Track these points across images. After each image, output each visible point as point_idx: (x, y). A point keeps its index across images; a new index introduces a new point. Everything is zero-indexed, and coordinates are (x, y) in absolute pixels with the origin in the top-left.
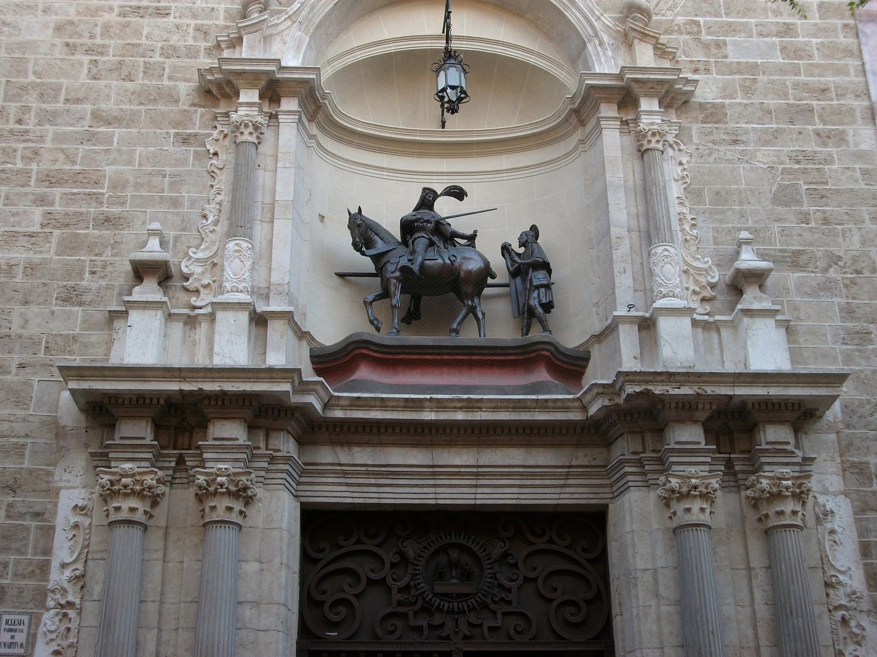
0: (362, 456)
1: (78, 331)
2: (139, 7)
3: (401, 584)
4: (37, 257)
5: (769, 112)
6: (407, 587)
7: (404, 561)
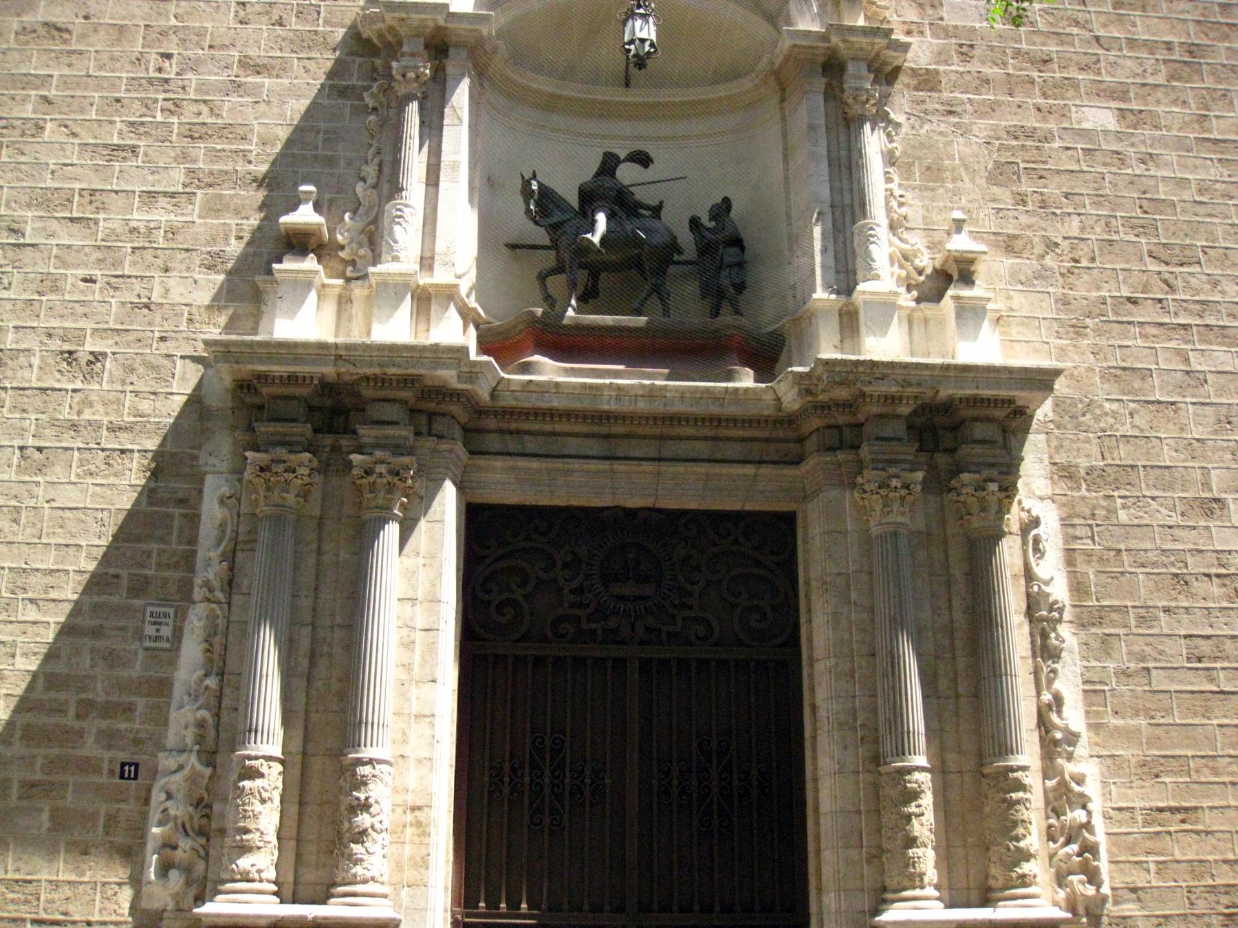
3: (574, 585)
5: (987, 81)
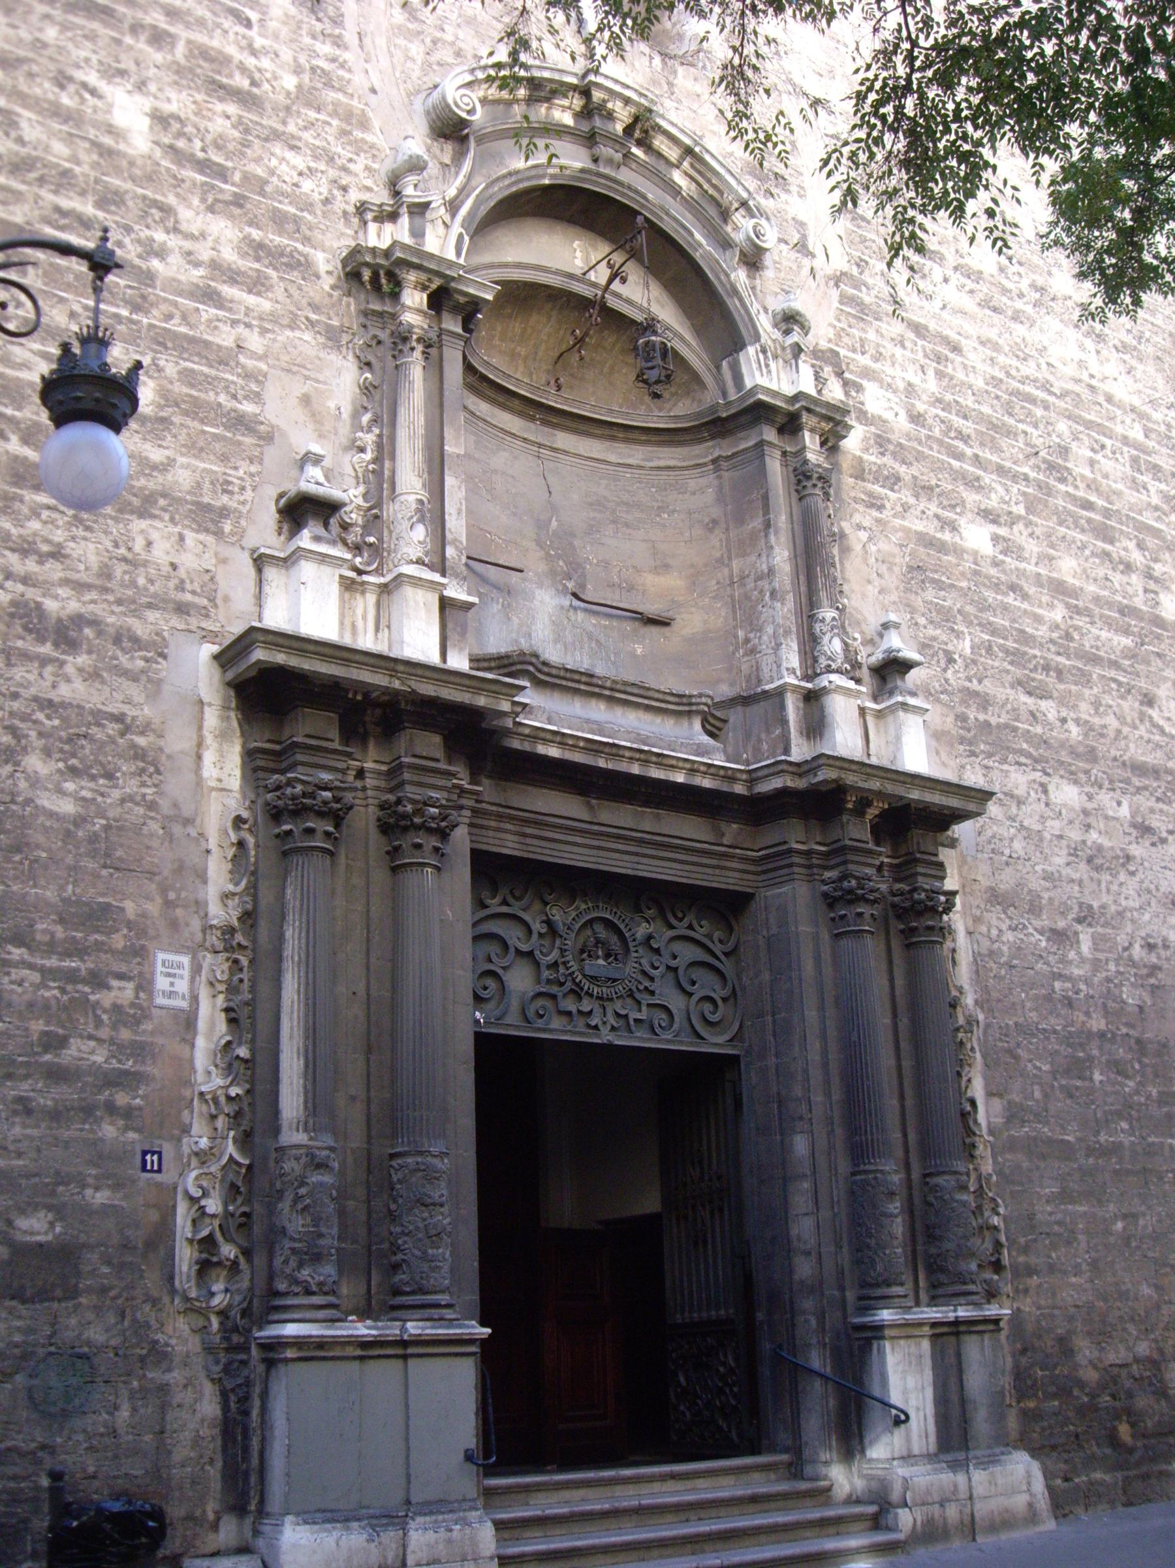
3: (550, 958)
7: (552, 930)
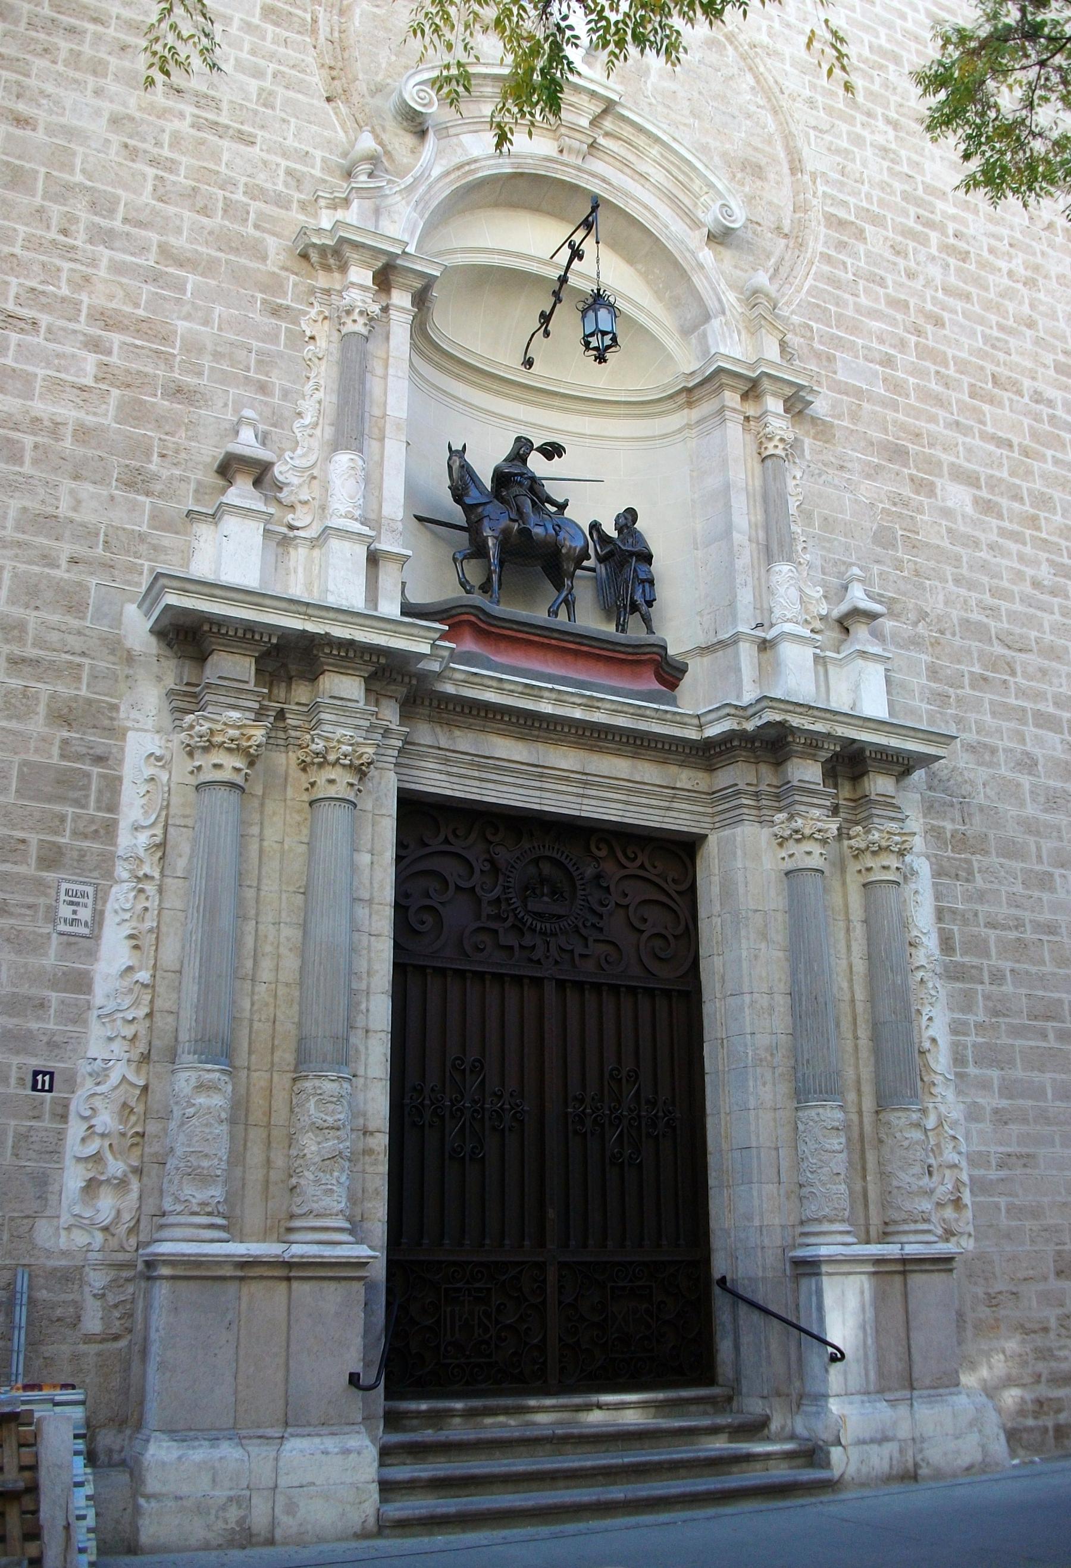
0: (465, 741)
1: (145, 528)
2: (217, 123)
4: (90, 420)
5: (872, 444)
6: (498, 900)
